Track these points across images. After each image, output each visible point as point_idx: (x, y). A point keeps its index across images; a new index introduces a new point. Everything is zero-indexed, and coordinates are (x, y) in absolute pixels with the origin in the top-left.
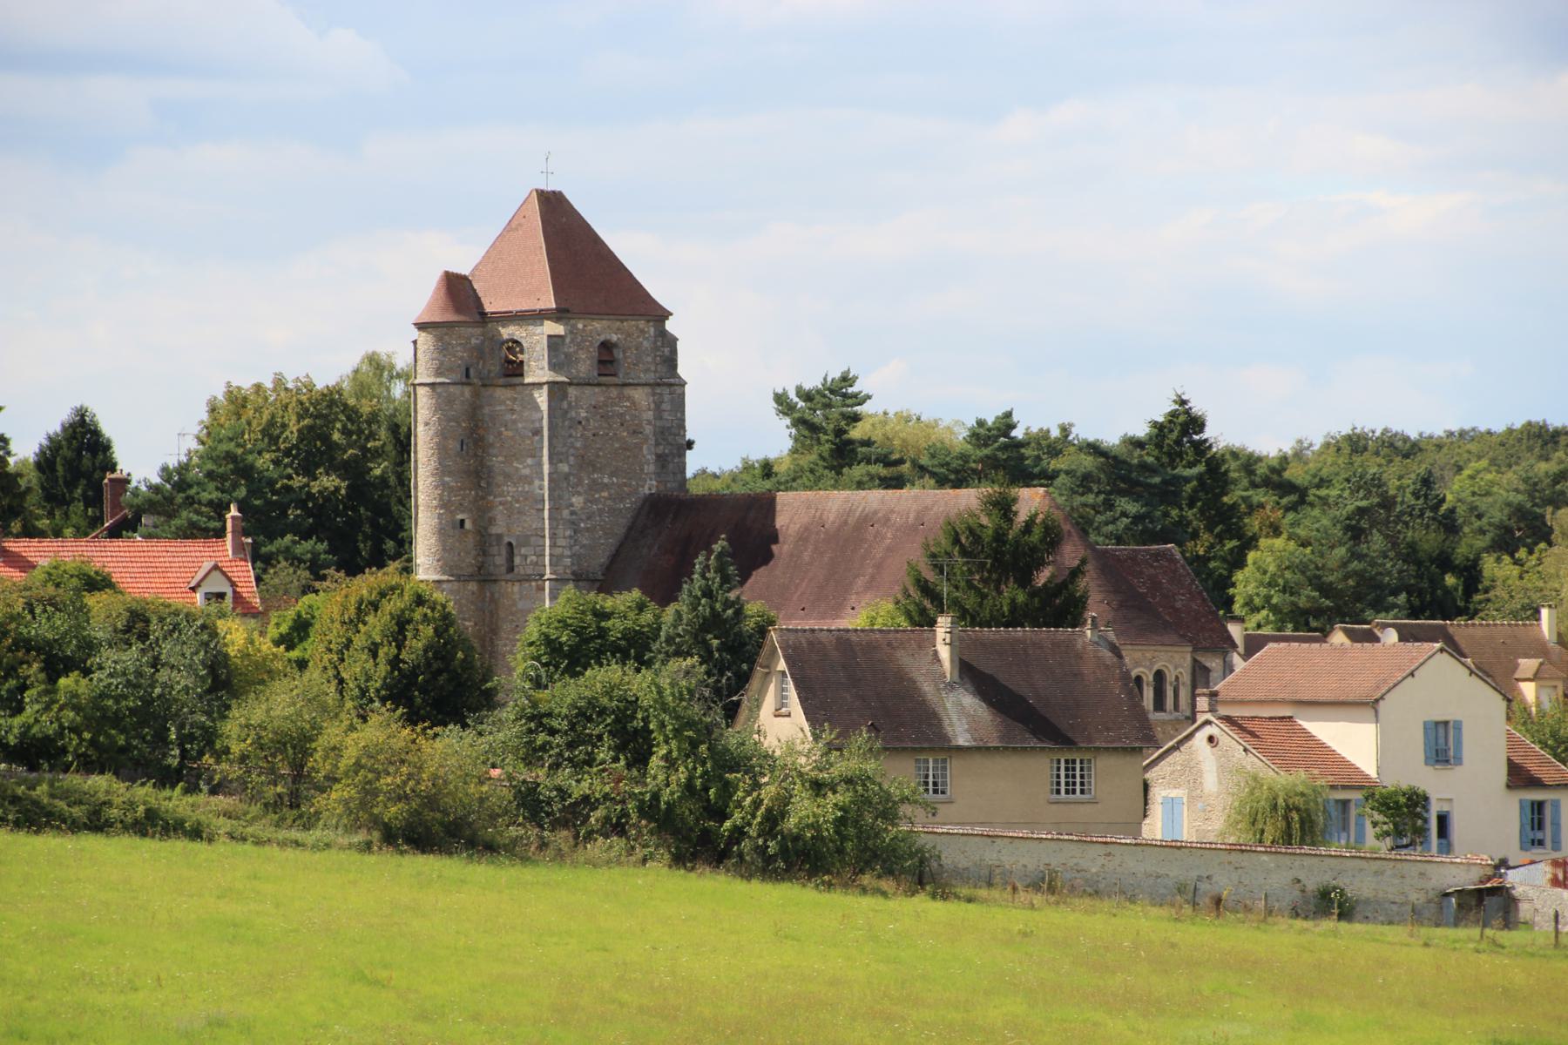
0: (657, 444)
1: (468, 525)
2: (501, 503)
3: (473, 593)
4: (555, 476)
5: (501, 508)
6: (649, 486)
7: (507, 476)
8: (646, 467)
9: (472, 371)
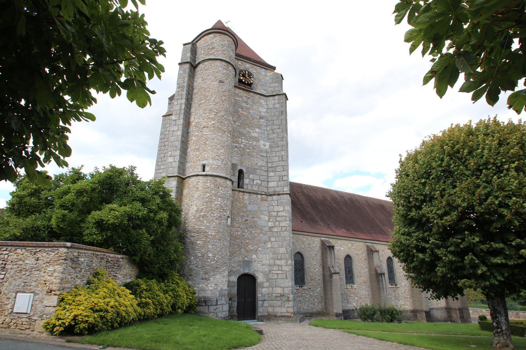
2: (236, 147)
5: (236, 149)
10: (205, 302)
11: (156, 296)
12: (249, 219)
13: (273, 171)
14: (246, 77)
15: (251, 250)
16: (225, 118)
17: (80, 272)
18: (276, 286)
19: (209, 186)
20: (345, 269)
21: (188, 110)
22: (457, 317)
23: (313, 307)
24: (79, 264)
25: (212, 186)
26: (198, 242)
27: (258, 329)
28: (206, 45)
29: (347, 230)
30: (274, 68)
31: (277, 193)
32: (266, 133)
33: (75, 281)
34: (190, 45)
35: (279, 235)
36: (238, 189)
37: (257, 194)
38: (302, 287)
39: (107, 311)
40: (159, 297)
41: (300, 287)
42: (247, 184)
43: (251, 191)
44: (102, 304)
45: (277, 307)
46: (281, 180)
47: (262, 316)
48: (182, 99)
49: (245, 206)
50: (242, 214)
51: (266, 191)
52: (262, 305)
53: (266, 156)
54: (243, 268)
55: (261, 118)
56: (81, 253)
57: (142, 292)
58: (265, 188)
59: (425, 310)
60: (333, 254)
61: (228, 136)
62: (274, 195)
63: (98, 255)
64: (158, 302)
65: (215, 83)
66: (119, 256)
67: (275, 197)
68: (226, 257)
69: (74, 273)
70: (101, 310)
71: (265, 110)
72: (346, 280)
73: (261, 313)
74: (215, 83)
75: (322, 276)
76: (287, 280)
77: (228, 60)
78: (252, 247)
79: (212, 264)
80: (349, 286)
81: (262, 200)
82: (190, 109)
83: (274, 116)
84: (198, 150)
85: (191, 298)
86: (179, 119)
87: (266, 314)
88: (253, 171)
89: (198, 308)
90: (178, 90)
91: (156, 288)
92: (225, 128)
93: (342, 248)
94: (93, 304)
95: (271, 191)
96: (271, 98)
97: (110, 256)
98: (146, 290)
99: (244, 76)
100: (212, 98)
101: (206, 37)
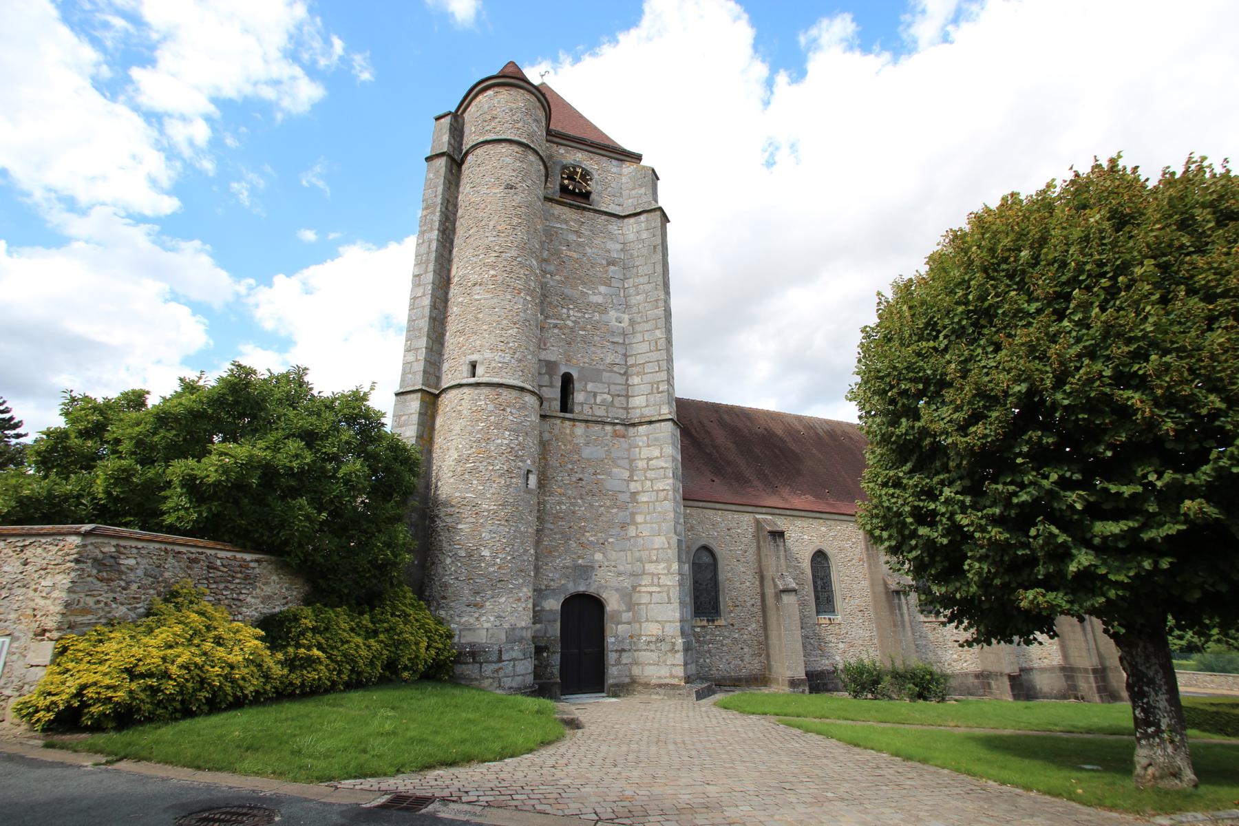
2: (555, 326)
5: (556, 331)
10: (475, 654)
11: (339, 644)
12: (586, 476)
13: (638, 374)
14: (574, 180)
15: (592, 542)
16: (520, 263)
17: (124, 589)
18: (647, 620)
19: (484, 407)
20: (815, 582)
21: (446, 254)
22: (1090, 688)
23: (739, 666)
24: (121, 572)
25: (491, 407)
26: (460, 526)
27: (565, 717)
28: (479, 114)
29: (816, 496)
30: (637, 158)
31: (648, 419)
32: (622, 295)
33: (107, 609)
34: (448, 118)
35: (651, 508)
36: (562, 415)
37: (604, 423)
38: (713, 621)
39: (166, 675)
40: (346, 646)
41: (708, 621)
42: (582, 404)
43: (589, 418)
44: (154, 660)
45: (650, 664)
46: (655, 391)
47: (616, 685)
48: (432, 229)
49: (577, 449)
50: (570, 466)
51: (625, 417)
52: (618, 662)
53: (624, 343)
54: (574, 581)
55: (611, 263)
56: (125, 547)
57: (303, 633)
58: (621, 411)
59: (1007, 671)
60: (782, 548)
61: (525, 299)
62: (641, 424)
63: (179, 553)
64: (345, 655)
65: (498, 191)
66: (248, 557)
67: (642, 429)
68: (526, 558)
69: (106, 592)
70: (150, 675)
71: (619, 247)
72: (817, 605)
73: (615, 678)
74: (498, 191)
75: (758, 597)
76: (671, 607)
77: (524, 141)
78: (595, 535)
79: (491, 573)
80: (824, 619)
81: (616, 435)
82: (451, 252)
83: (638, 256)
84: (462, 332)
85: (441, 646)
86: (426, 272)
87: (627, 680)
88: (596, 375)
89: (459, 669)
90: (425, 212)
91: (343, 625)
92: (519, 284)
94: (132, 659)
95: (635, 416)
96: (632, 220)
97: (219, 556)
98: (315, 630)
99: (571, 178)
100: (492, 223)
101: (480, 97)
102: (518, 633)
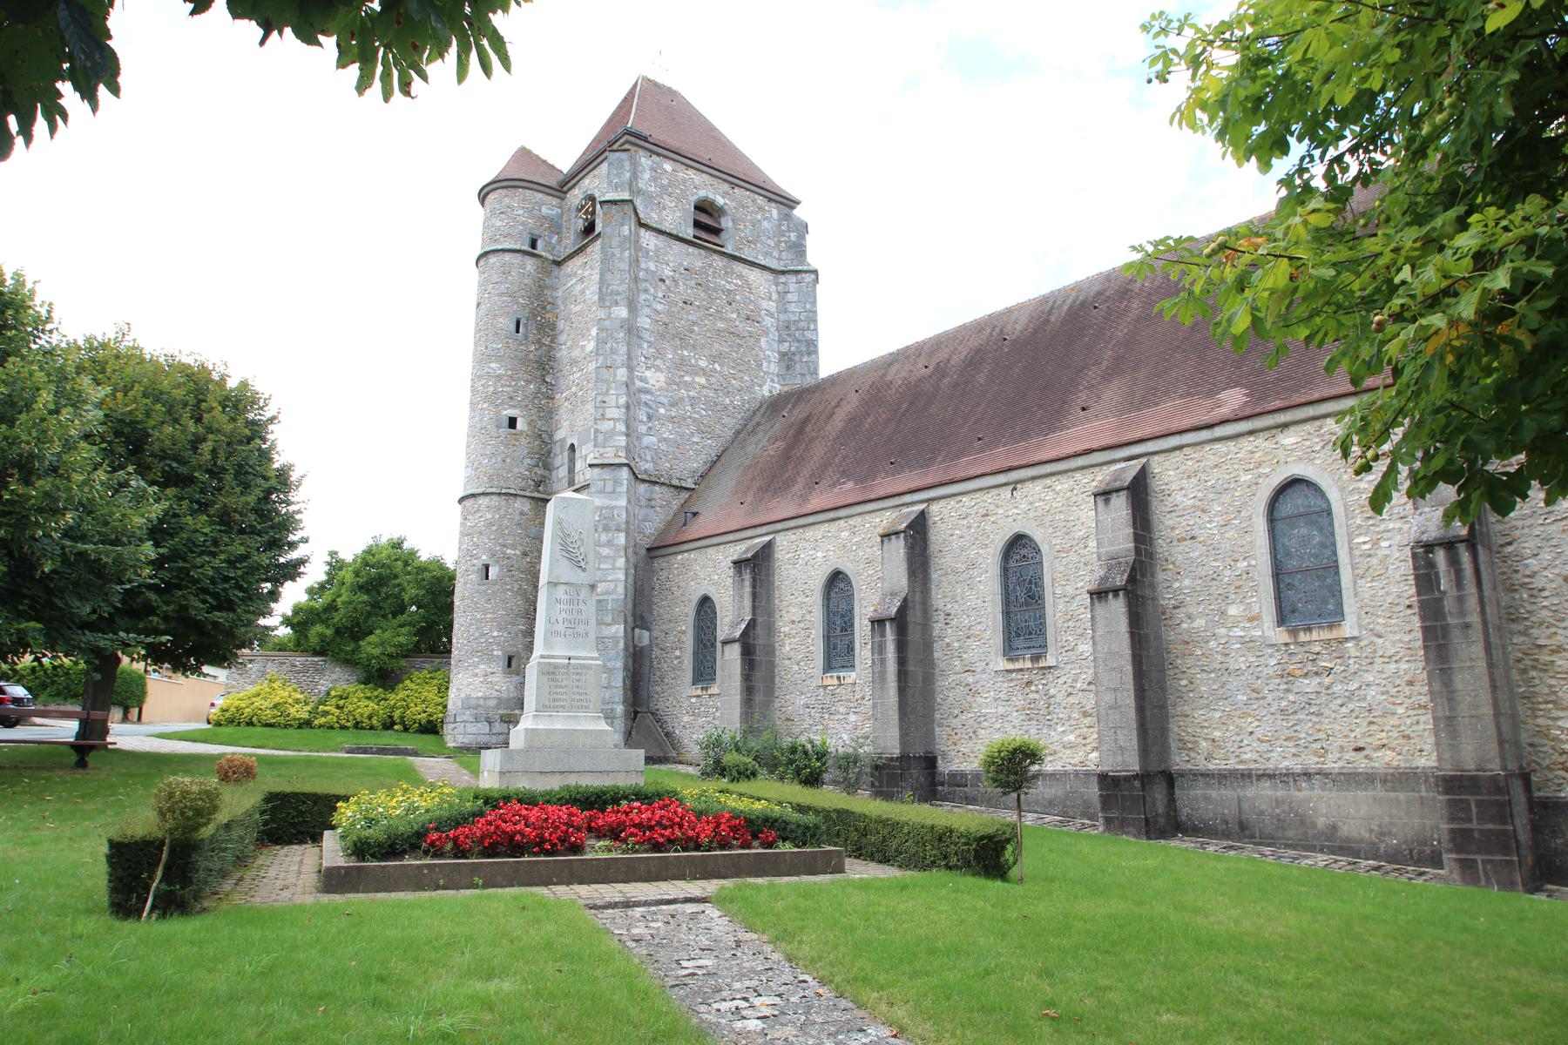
0: (781, 341)
1: (520, 424)
3: (522, 513)
4: (607, 323)
5: (566, 404)
6: (770, 387)
7: (573, 362)
8: (765, 364)
9: (540, 243)
38: (706, 689)
41: (702, 688)
66: (316, 659)
93: (820, 554)
102: (473, 702)
